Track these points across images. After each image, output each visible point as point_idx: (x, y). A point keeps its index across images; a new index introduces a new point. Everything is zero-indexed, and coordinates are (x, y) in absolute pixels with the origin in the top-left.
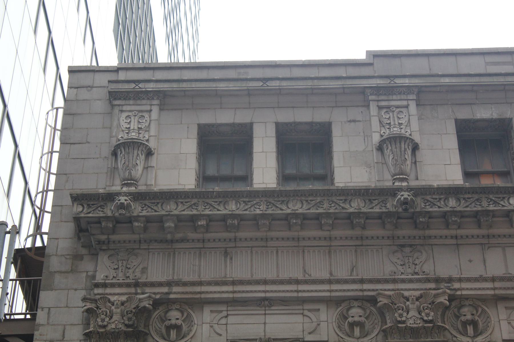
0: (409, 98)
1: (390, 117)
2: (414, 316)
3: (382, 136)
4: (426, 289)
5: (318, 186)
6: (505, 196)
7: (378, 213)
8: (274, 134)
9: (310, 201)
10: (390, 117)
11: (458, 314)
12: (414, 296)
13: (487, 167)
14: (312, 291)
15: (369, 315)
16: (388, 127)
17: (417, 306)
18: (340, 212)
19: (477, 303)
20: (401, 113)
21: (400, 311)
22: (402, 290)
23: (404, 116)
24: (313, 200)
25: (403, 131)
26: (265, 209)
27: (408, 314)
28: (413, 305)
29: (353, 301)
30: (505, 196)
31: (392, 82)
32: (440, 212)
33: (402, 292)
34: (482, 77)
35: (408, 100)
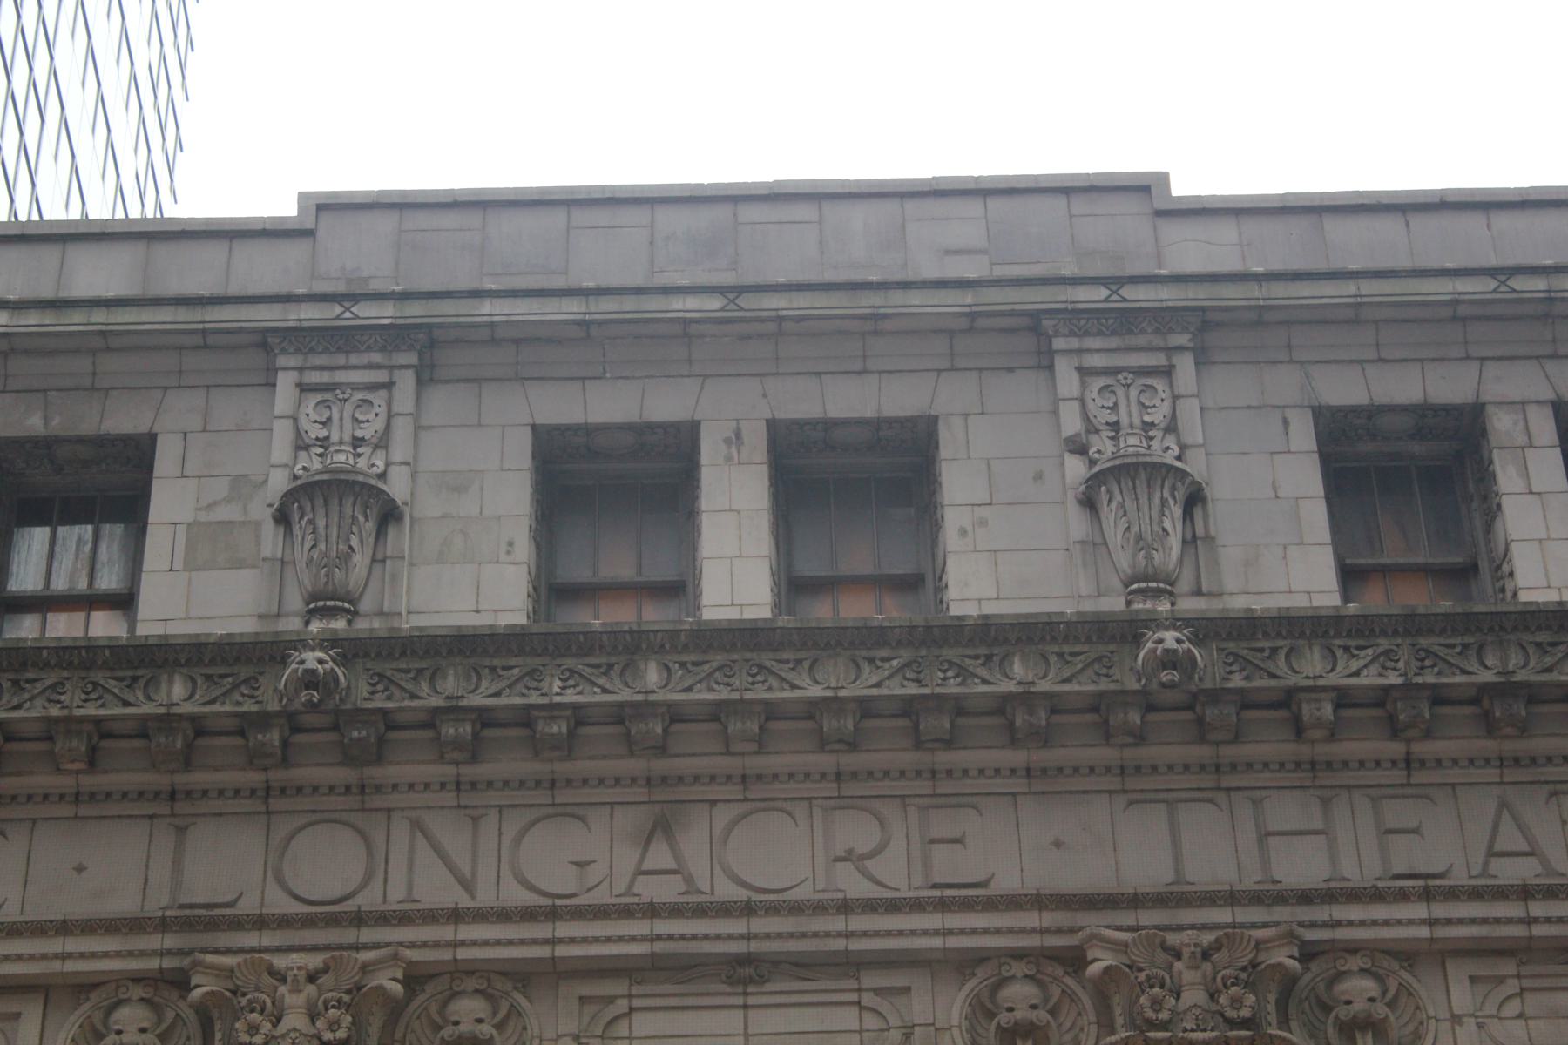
0: (394, 362)
1: (329, 419)
2: (295, 1030)
3: (295, 477)
4: (340, 947)
5: (655, 615)
6: (613, 659)
7: (514, 707)
8: (526, 462)
9: (694, 664)
10: (329, 419)
11: (990, 1006)
12: (299, 968)
13: (858, 560)
14: (621, 939)
15: (173, 1026)
16: (320, 450)
17: (308, 1000)
18: (401, 709)
19: (499, 986)
20: (365, 407)
21: (255, 1015)
22: (267, 950)
23: (371, 416)
24: (226, 676)
25: (362, 463)
26: (77, 702)
27: (275, 1026)
28: (294, 997)
29: (130, 984)
30: (613, 659)
31: (347, 315)
32: (992, 695)
33: (266, 956)
34: (644, 297)
35: (391, 368)
